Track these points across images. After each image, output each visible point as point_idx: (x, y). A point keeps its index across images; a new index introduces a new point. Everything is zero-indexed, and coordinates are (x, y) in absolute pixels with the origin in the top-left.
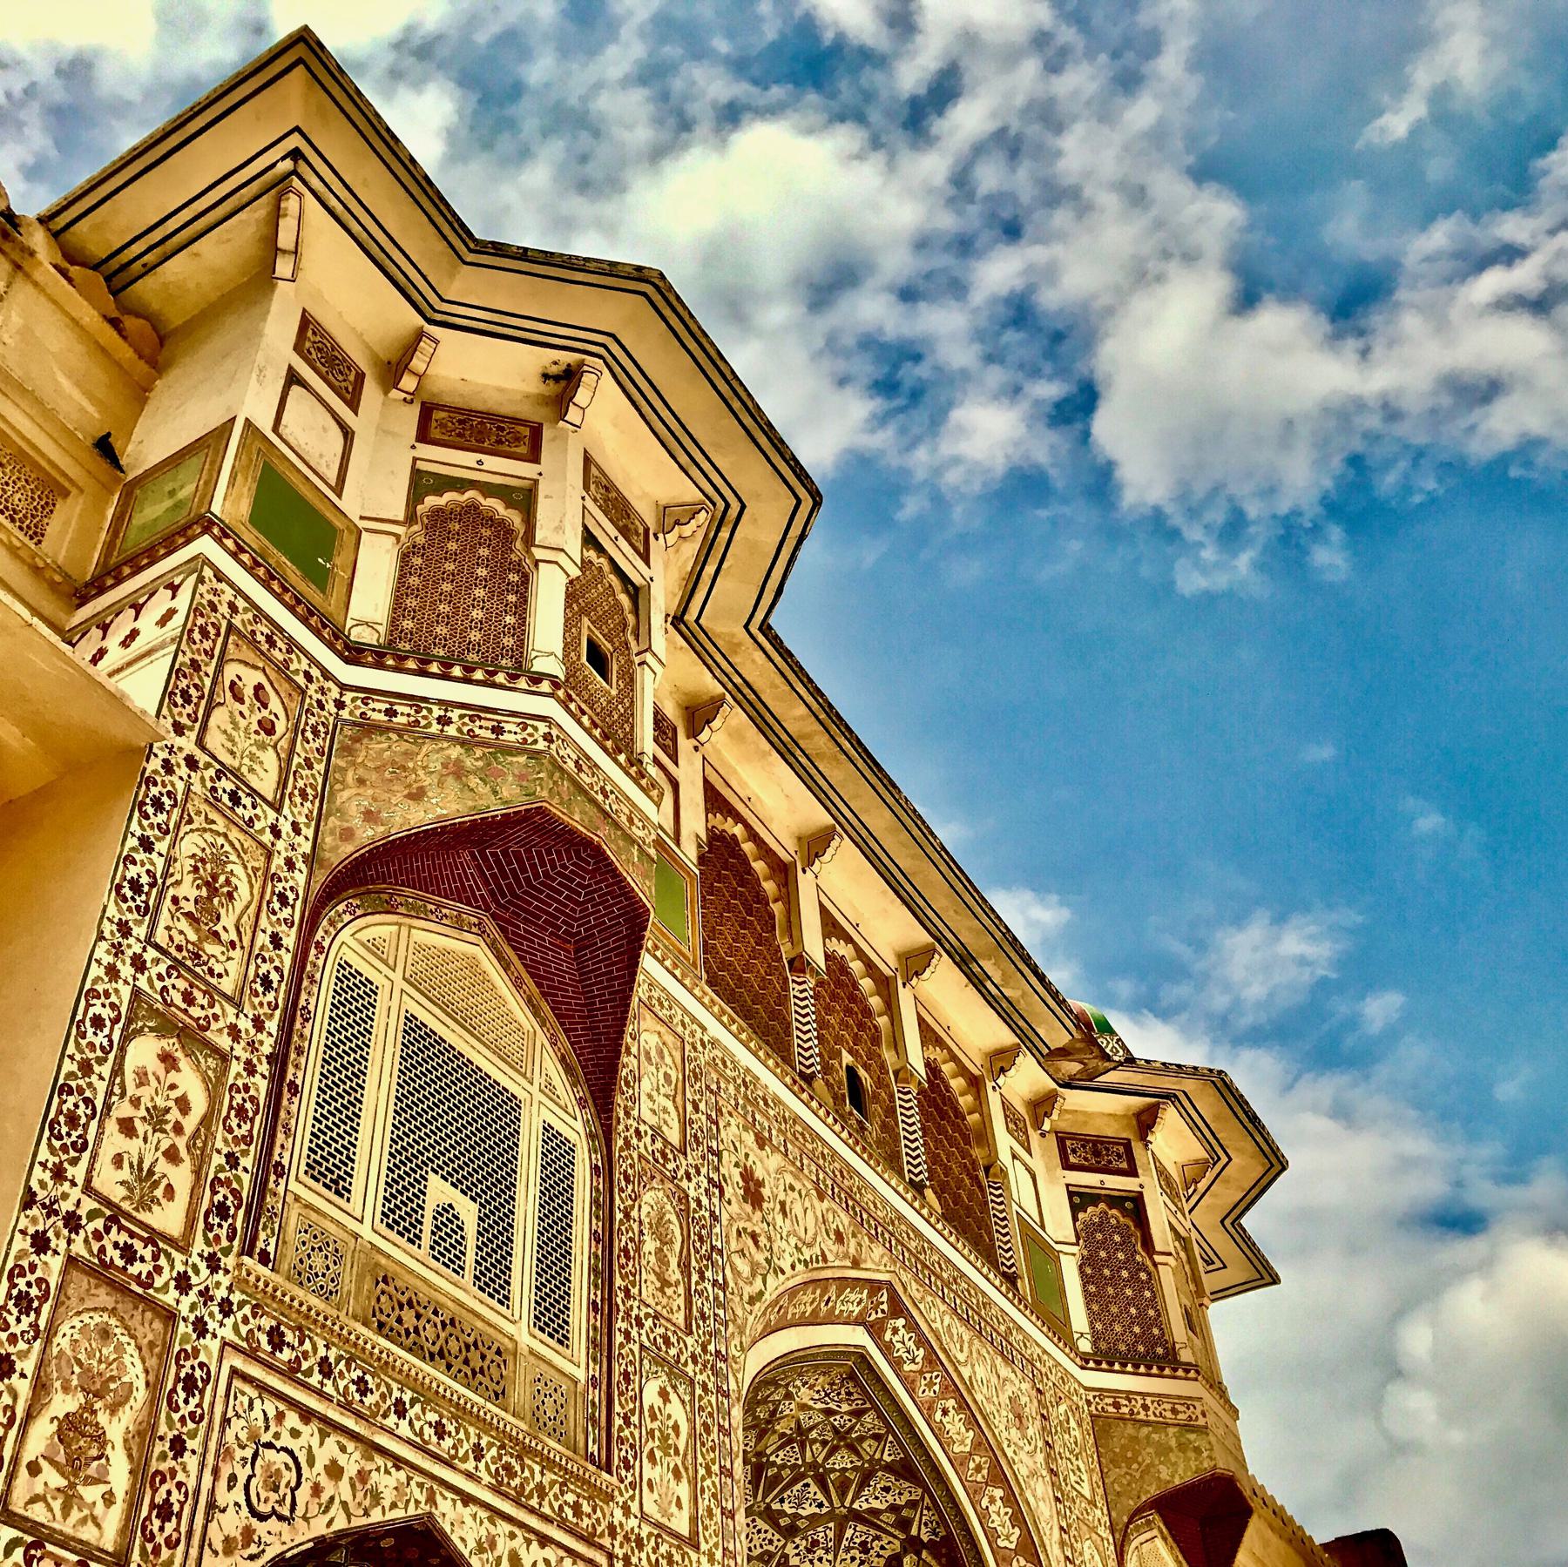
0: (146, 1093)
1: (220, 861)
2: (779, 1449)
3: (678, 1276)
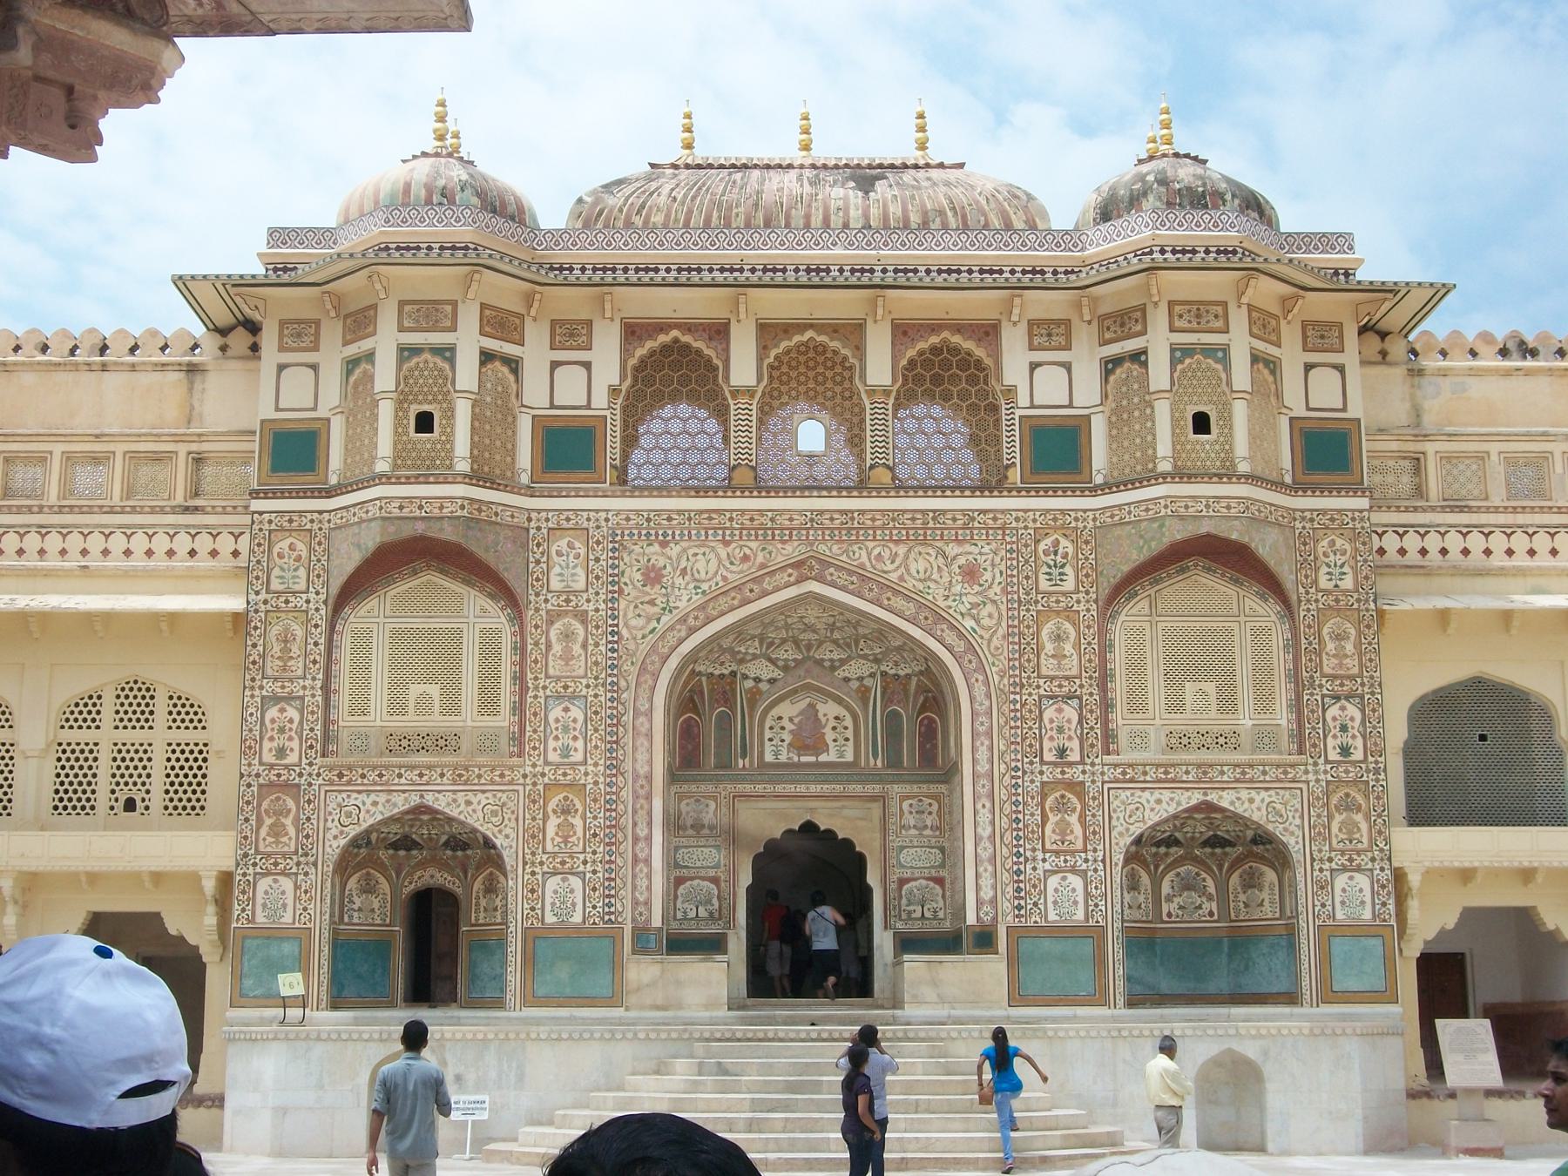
1: (286, 630)
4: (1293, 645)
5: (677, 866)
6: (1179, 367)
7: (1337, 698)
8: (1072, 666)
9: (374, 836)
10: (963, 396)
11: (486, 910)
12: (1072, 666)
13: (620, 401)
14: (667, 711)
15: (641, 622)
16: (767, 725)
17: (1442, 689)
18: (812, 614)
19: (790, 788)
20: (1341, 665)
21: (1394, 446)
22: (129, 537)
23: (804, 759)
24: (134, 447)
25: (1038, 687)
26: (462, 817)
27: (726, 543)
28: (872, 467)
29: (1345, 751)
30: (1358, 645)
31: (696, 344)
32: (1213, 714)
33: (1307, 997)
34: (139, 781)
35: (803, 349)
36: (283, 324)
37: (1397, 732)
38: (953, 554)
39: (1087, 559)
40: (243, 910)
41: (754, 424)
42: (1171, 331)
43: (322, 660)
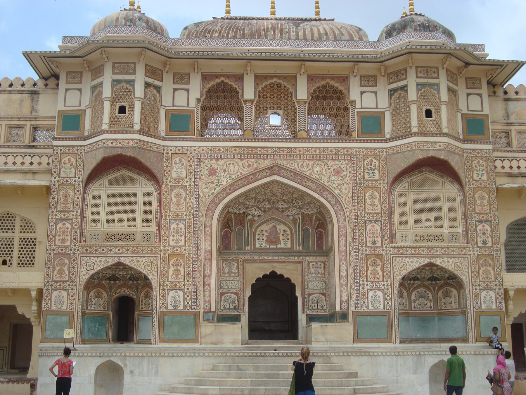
0: (61, 230)
1: (66, 192)
2: (283, 196)
3: (183, 201)
4: (464, 201)
5: (221, 288)
6: (420, 92)
7: (481, 222)
8: (378, 209)
9: (100, 275)
10: (335, 104)
11: (145, 305)
12: (378, 209)
13: (200, 105)
14: (218, 226)
15: (208, 190)
16: (257, 233)
17: (519, 220)
18: (275, 189)
19: (266, 258)
20: (482, 209)
21: (499, 127)
22: (6, 157)
23: (271, 247)
24: (9, 122)
25: (365, 217)
26: (135, 267)
27: (242, 160)
28: (299, 131)
29: (484, 242)
30: (489, 201)
31: (230, 83)
32: (433, 228)
33: (471, 339)
34: (8, 253)
35: (272, 85)
36: (68, 73)
37: (503, 237)
38: (331, 164)
39: (383, 167)
40: (47, 304)
41: (253, 114)
42: (417, 77)
43: (80, 204)
